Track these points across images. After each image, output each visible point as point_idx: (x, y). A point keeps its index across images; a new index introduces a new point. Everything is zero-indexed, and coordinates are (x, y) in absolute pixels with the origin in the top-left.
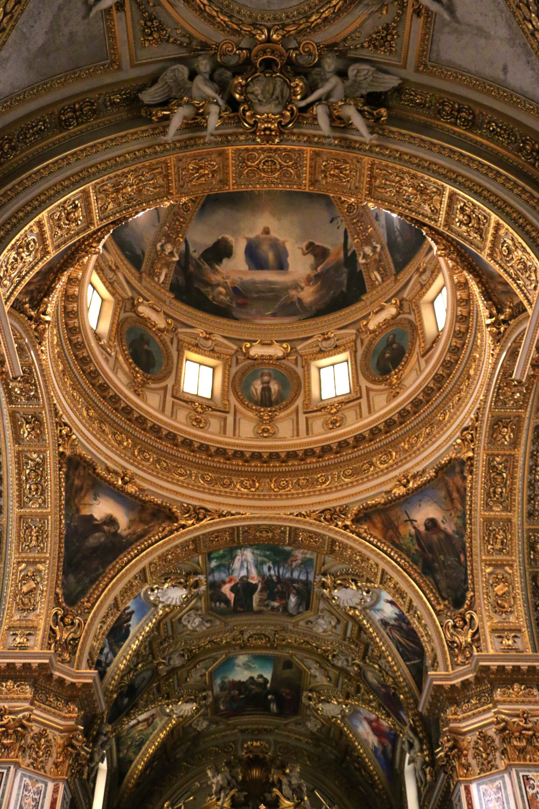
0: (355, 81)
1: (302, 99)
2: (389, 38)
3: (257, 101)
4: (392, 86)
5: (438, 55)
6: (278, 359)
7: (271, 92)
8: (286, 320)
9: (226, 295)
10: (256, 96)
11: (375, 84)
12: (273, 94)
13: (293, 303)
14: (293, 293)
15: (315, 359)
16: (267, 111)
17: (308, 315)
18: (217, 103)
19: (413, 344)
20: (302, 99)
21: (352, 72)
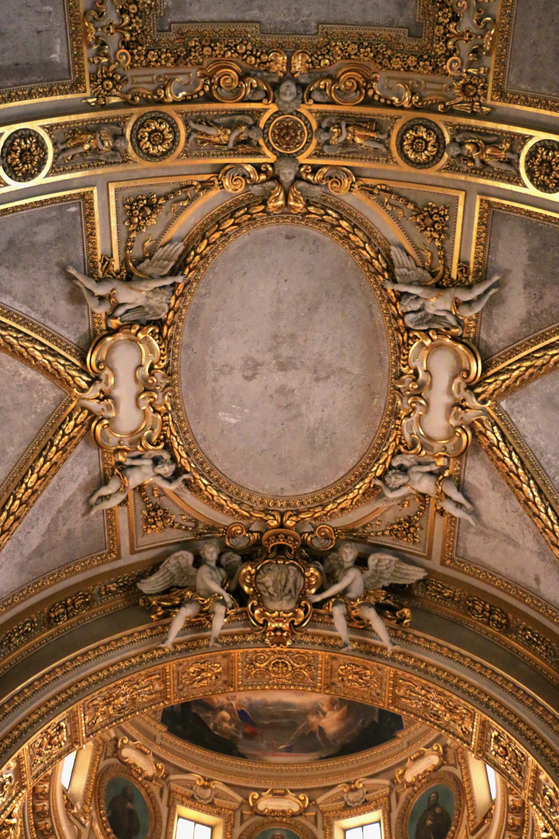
0: (376, 571)
1: (318, 593)
2: (412, 530)
3: (267, 594)
4: (416, 578)
5: (465, 551)
6: (293, 815)
7: (283, 583)
8: (305, 758)
9: (230, 723)
10: (267, 588)
11: (398, 575)
12: (285, 586)
13: (312, 734)
14: (313, 719)
15: (339, 818)
16: (278, 608)
17: (332, 751)
18: (223, 602)
19: (460, 813)
20: (318, 593)
21: (372, 561)
